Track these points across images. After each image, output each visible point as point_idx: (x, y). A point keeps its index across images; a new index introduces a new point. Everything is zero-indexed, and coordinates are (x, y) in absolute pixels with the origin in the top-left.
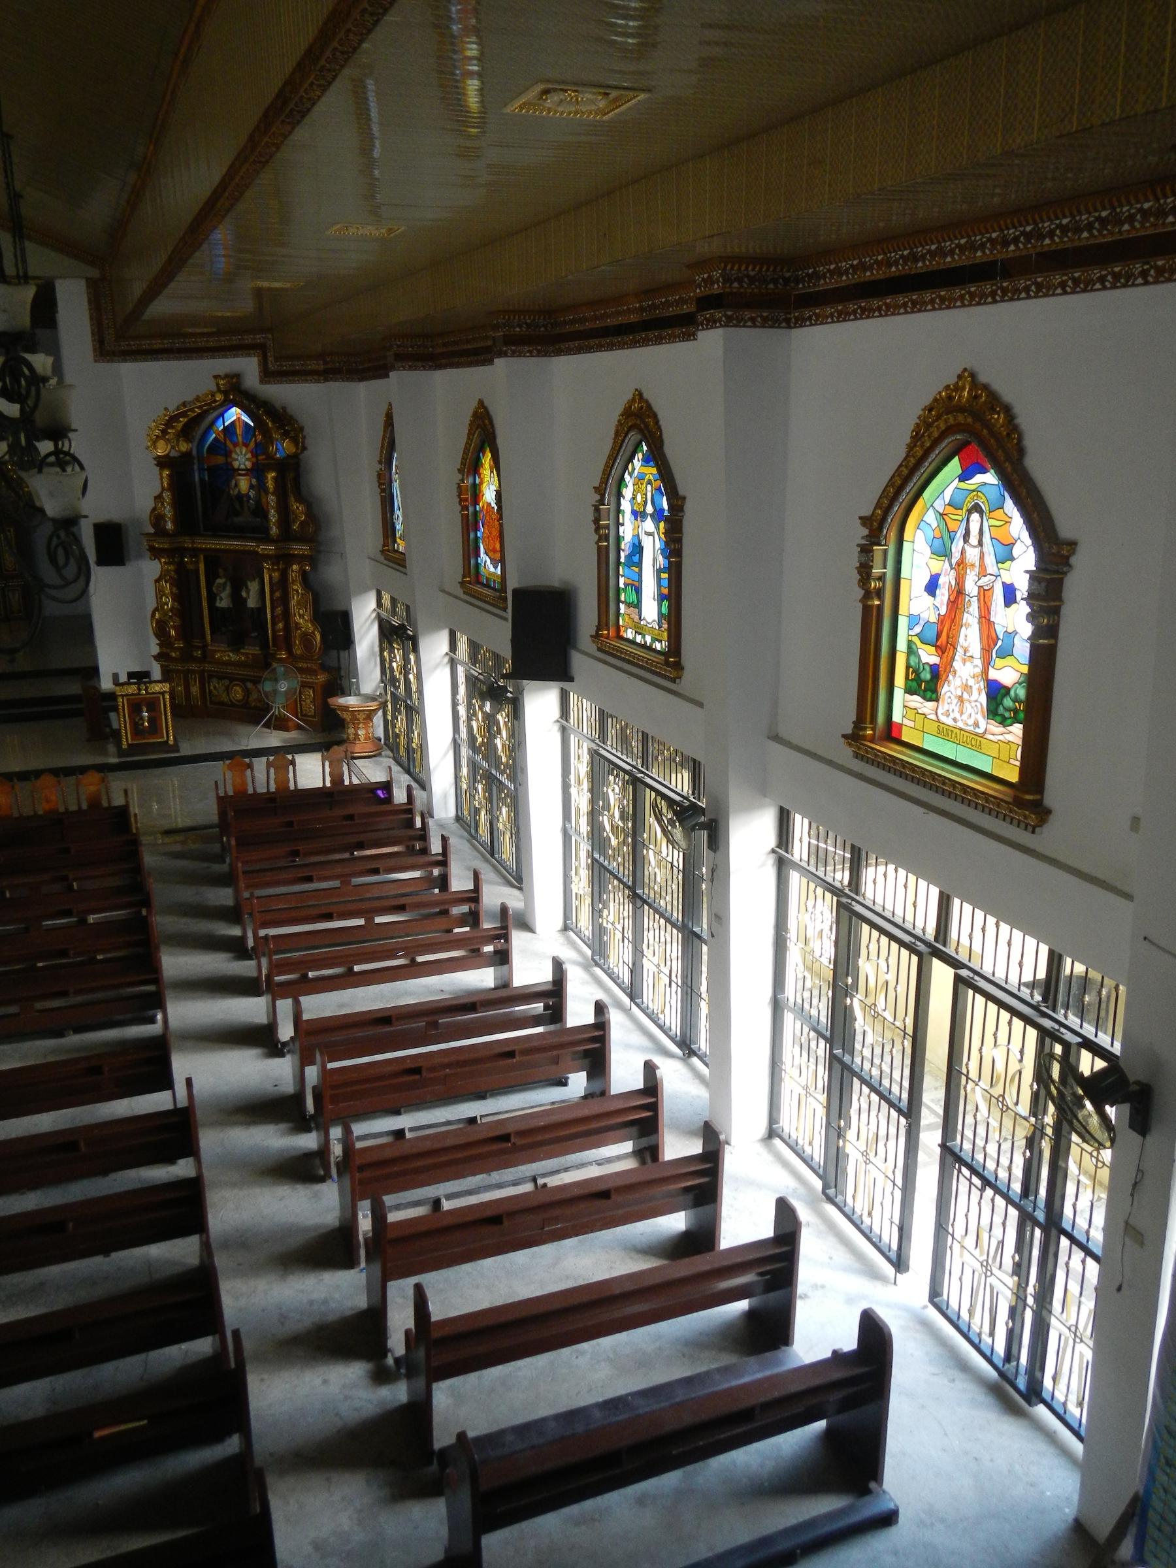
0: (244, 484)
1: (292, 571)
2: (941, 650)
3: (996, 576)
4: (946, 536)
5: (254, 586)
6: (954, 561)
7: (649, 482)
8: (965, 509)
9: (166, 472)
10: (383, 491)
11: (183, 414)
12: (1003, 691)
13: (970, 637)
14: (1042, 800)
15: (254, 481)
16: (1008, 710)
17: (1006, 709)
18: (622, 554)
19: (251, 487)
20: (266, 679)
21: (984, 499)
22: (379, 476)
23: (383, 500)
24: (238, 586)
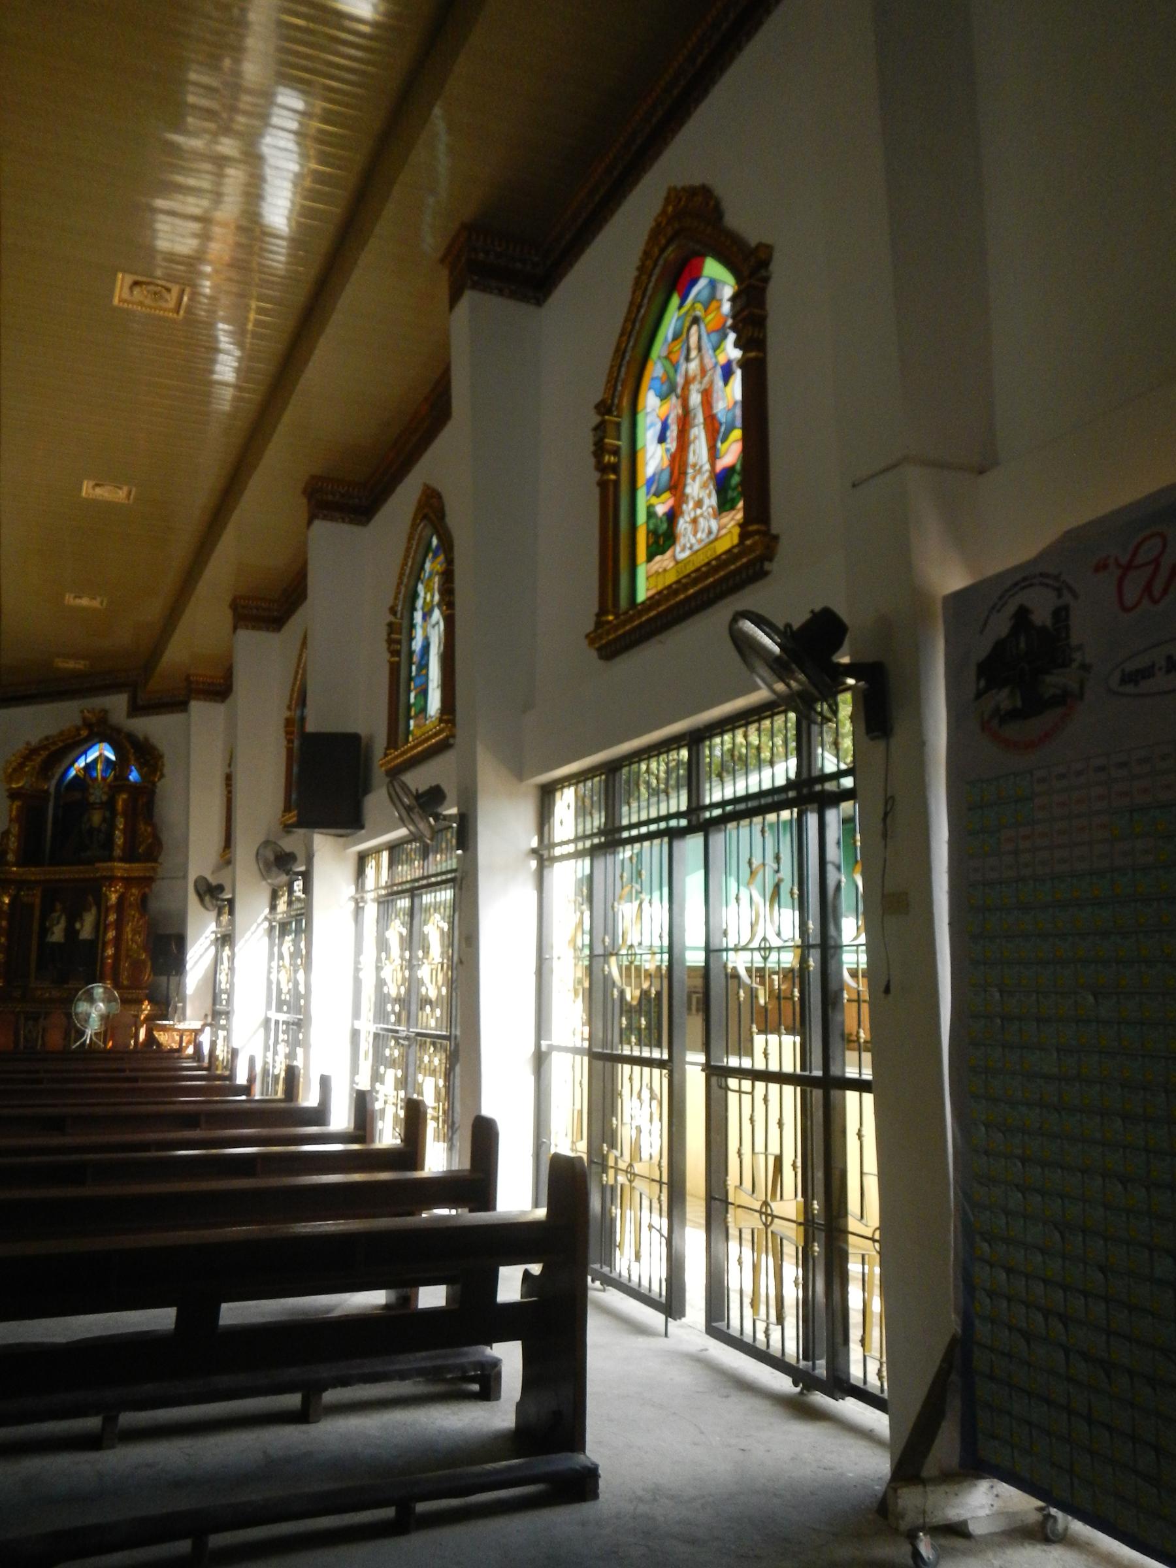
1: (132, 895)
5: (89, 919)
9: (17, 803)
11: (45, 748)
14: (769, 530)
15: (108, 814)
19: (104, 820)
20: (79, 1000)
24: (74, 916)
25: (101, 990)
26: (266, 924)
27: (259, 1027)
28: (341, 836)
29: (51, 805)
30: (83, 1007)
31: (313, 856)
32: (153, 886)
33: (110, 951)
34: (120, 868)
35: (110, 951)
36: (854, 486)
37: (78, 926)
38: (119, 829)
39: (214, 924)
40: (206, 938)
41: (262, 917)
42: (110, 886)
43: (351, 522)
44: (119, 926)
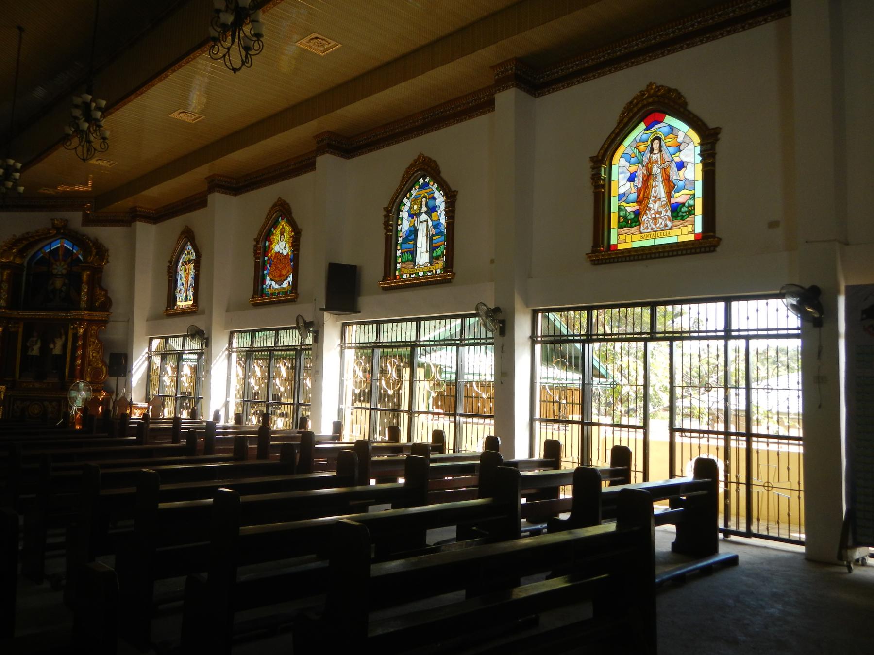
0: (59, 283)
1: (92, 330)
2: (639, 201)
3: (671, 161)
4: (639, 155)
5: (59, 343)
6: (645, 164)
7: (425, 197)
8: (650, 140)
10: (170, 276)
12: (681, 206)
13: (660, 190)
15: (66, 281)
16: (685, 212)
17: (683, 213)
18: (400, 239)
21: (660, 133)
22: (169, 268)
23: (169, 280)
25: (83, 385)
26: (227, 352)
27: (223, 407)
28: (336, 315)
29: (25, 273)
30: (74, 394)
31: (324, 324)
32: (107, 325)
33: (79, 362)
34: (86, 315)
35: (79, 362)
36: (807, 242)
37: (52, 346)
38: (84, 291)
39: (147, 349)
40: (143, 356)
41: (225, 348)
42: (80, 324)
43: (342, 156)
44: (84, 347)
